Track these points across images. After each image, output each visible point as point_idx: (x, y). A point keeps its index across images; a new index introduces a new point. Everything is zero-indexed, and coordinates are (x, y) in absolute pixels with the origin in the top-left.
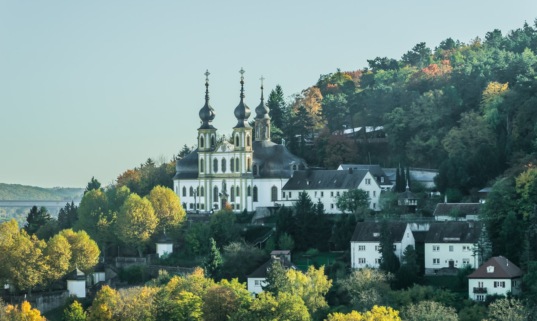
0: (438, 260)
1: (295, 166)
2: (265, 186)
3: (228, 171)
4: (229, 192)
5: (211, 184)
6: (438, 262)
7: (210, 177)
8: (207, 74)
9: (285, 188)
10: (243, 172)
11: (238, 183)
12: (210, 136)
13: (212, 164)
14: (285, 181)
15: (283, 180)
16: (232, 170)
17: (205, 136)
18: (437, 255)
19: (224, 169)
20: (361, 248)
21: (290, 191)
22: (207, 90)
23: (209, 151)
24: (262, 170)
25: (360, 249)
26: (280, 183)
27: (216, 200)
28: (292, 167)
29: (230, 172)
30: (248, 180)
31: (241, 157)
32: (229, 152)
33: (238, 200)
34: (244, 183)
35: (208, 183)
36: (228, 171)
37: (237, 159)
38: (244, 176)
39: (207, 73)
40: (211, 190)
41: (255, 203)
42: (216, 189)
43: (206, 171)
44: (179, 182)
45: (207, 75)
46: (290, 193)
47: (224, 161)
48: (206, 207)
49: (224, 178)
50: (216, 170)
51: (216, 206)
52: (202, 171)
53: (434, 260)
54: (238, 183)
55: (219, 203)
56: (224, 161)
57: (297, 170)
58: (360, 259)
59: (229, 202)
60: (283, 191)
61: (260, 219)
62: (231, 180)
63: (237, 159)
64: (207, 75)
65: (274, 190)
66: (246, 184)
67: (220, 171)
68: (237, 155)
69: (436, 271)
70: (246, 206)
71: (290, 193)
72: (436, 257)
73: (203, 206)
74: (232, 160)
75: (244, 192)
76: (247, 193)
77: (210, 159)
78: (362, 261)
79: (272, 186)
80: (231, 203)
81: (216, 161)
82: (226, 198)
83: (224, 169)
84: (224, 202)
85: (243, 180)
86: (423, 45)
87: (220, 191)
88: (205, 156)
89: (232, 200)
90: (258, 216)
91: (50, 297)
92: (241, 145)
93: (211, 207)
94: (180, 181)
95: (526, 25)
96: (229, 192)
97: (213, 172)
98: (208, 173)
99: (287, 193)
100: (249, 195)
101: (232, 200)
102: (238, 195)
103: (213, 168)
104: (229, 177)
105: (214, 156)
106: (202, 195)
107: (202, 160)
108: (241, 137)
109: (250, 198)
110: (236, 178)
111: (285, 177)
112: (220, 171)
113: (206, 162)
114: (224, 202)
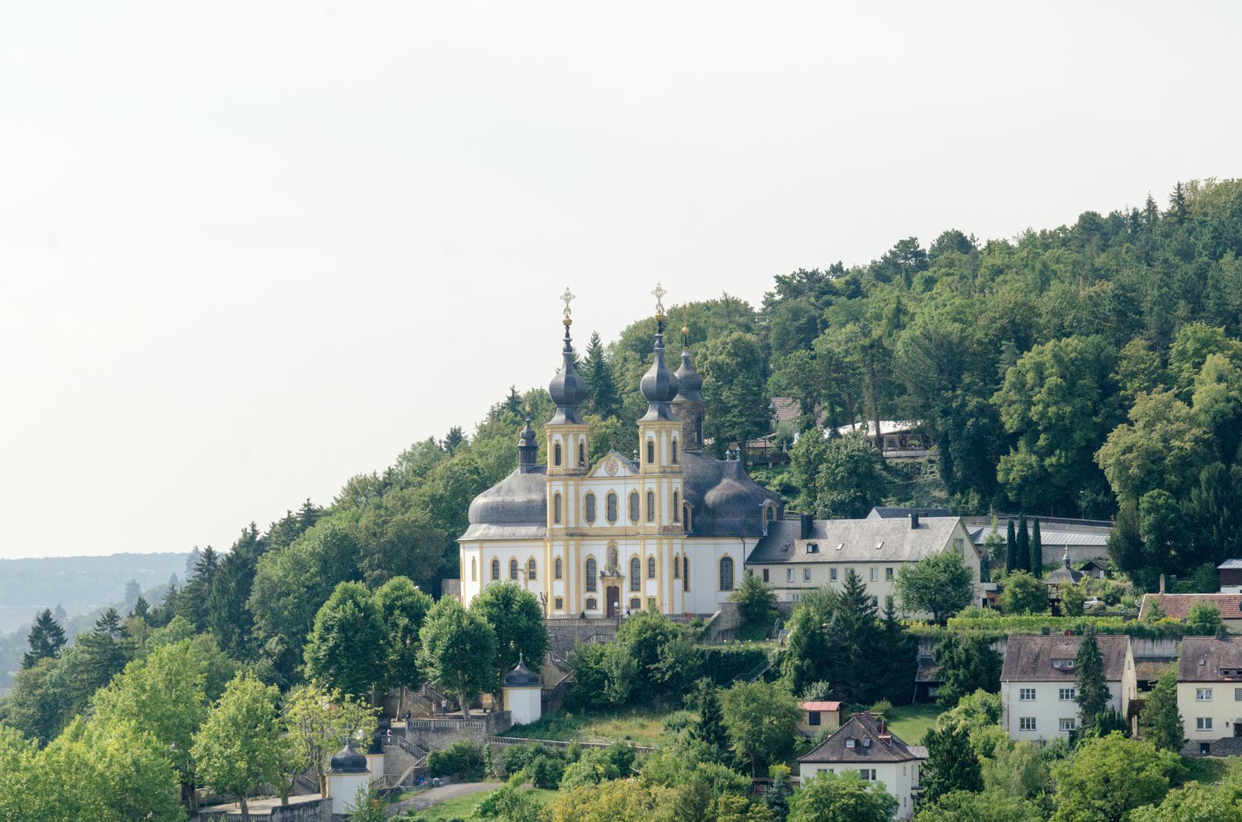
0: (1209, 721)
1: (770, 509)
2: (706, 554)
3: (623, 519)
4: (624, 568)
5: (578, 551)
6: (1209, 725)
7: (575, 535)
8: (567, 297)
9: (754, 559)
10: (666, 523)
11: (651, 549)
12: (576, 440)
13: (582, 504)
14: (751, 544)
15: (747, 541)
16: (634, 516)
17: (566, 441)
18: (1203, 709)
19: (612, 516)
20: (1028, 695)
21: (766, 567)
22: (568, 335)
23: (575, 475)
24: (697, 520)
25: (1022, 697)
26: (738, 550)
27: (591, 586)
28: (764, 512)
29: (629, 524)
30: (675, 541)
31: (660, 489)
32: (625, 477)
33: (650, 588)
34: (665, 548)
35: (572, 549)
36: (623, 519)
37: (650, 494)
38: (666, 532)
39: (567, 294)
40: (578, 566)
41: (686, 594)
42: (591, 564)
43: (567, 522)
44: (481, 548)
45: (568, 301)
46: (766, 572)
47: (612, 499)
48: (568, 603)
49: (612, 539)
50: (591, 517)
51: (591, 604)
52: (557, 521)
53: (1200, 721)
54: (651, 549)
55: (600, 595)
56: (612, 499)
57: (775, 519)
58: (1022, 720)
59: (626, 596)
60: (749, 567)
61: (727, 631)
62: (629, 542)
63: (650, 494)
64: (568, 301)
65: (726, 563)
66: (670, 550)
67: (601, 520)
68: (651, 485)
69: (1205, 746)
70: (672, 603)
71: (766, 572)
72: (1205, 715)
73: (559, 603)
74: (634, 497)
75: (665, 569)
76: (673, 573)
77: (577, 493)
78: (1028, 724)
79: (722, 555)
80: (633, 595)
81: (590, 499)
82: (617, 584)
83: (612, 516)
84: (613, 594)
85: (666, 541)
86: (913, 240)
87: (602, 565)
88: (566, 486)
89: (635, 586)
90: (725, 625)
91: (296, 813)
92: (660, 461)
93: (578, 604)
94: (485, 545)
95: (1150, 202)
96: (624, 568)
97: (584, 524)
98: (572, 524)
99: (758, 571)
100: (677, 576)
101: (635, 586)
102: (651, 575)
103: (583, 513)
104: (626, 535)
105: (588, 486)
106: (558, 576)
107: (557, 496)
108: (660, 444)
109: (679, 583)
110: (647, 536)
111: (751, 536)
112: (601, 520)
113: (567, 500)
114: (613, 594)
